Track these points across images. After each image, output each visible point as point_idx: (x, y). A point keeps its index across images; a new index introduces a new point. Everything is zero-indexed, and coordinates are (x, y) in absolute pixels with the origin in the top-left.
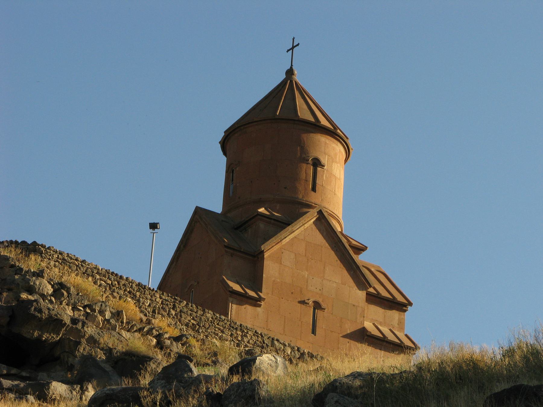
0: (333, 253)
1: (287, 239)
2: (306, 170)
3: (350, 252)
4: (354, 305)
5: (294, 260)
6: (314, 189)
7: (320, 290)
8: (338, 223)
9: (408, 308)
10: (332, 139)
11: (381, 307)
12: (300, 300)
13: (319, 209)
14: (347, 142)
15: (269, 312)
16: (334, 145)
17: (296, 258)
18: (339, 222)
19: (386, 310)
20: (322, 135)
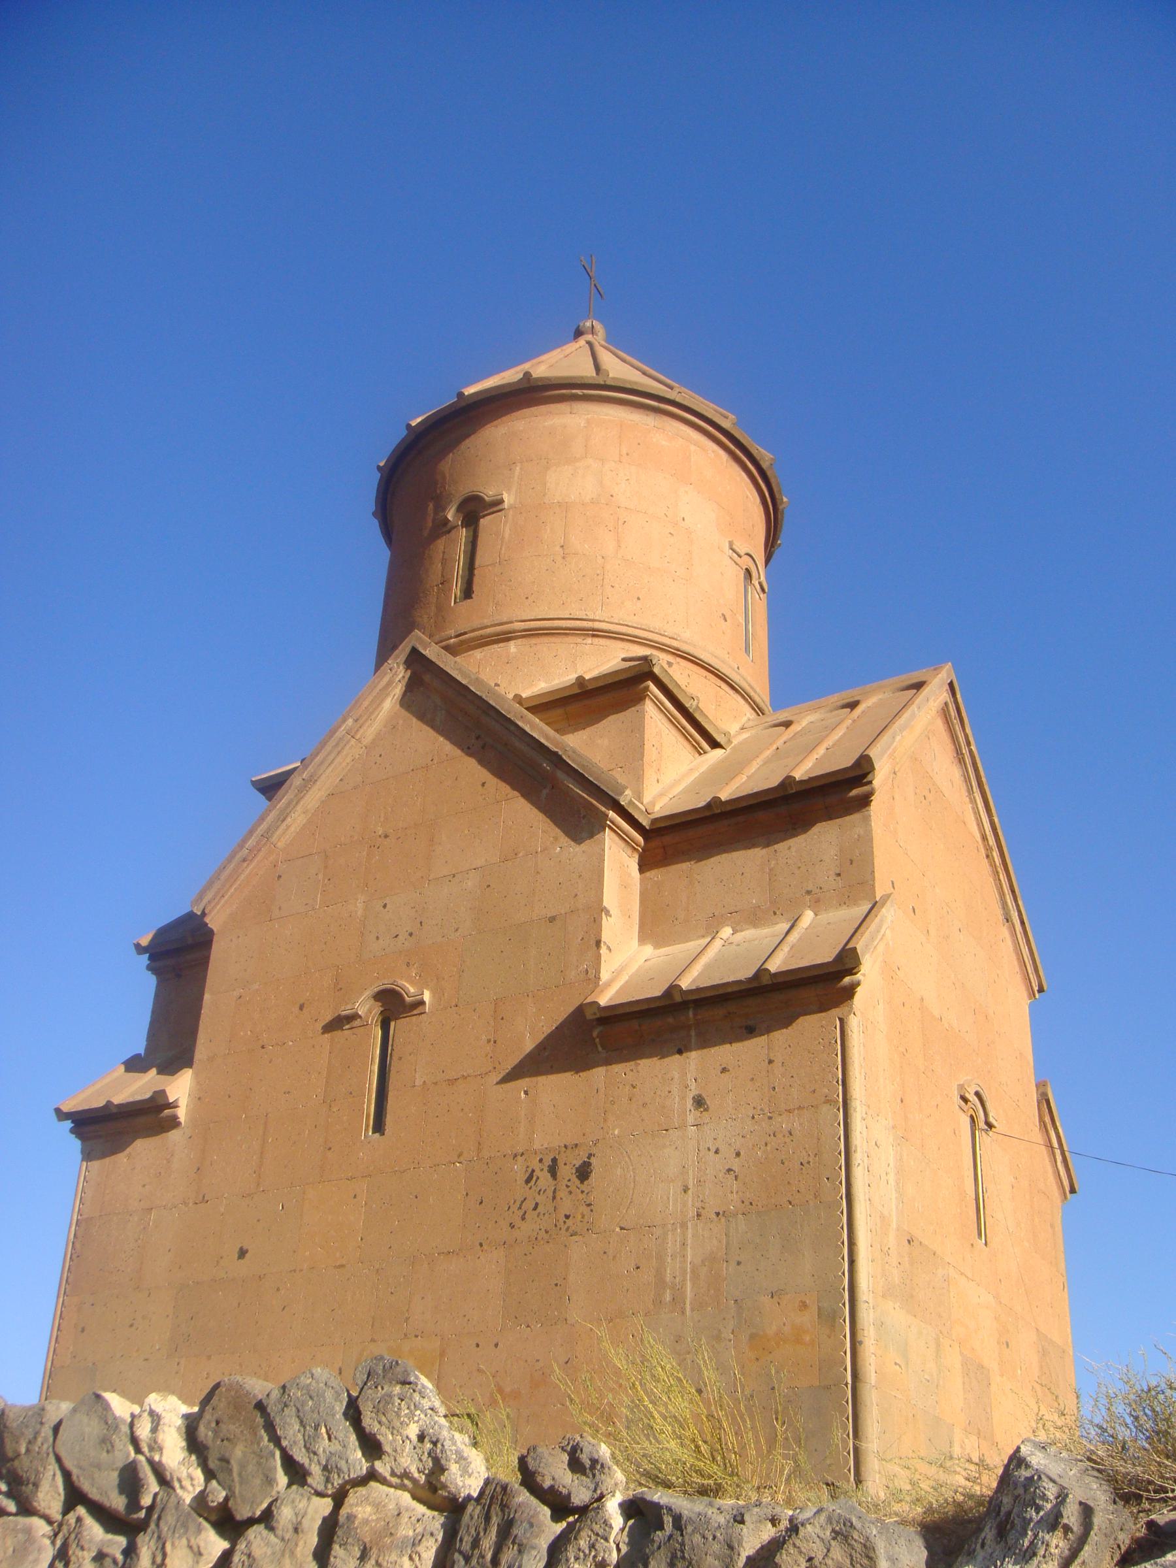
0: (472, 763)
1: (289, 819)
2: (444, 552)
3: (520, 724)
4: (552, 919)
5: (320, 876)
6: (468, 593)
7: (411, 934)
8: (594, 636)
9: (870, 782)
10: (543, 408)
11: (754, 846)
12: (328, 1017)
13: (408, 650)
14: (608, 383)
15: (211, 1125)
16: (548, 423)
17: (326, 867)
18: (595, 633)
19: (776, 846)
20: (496, 423)
